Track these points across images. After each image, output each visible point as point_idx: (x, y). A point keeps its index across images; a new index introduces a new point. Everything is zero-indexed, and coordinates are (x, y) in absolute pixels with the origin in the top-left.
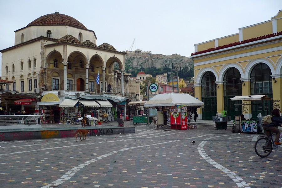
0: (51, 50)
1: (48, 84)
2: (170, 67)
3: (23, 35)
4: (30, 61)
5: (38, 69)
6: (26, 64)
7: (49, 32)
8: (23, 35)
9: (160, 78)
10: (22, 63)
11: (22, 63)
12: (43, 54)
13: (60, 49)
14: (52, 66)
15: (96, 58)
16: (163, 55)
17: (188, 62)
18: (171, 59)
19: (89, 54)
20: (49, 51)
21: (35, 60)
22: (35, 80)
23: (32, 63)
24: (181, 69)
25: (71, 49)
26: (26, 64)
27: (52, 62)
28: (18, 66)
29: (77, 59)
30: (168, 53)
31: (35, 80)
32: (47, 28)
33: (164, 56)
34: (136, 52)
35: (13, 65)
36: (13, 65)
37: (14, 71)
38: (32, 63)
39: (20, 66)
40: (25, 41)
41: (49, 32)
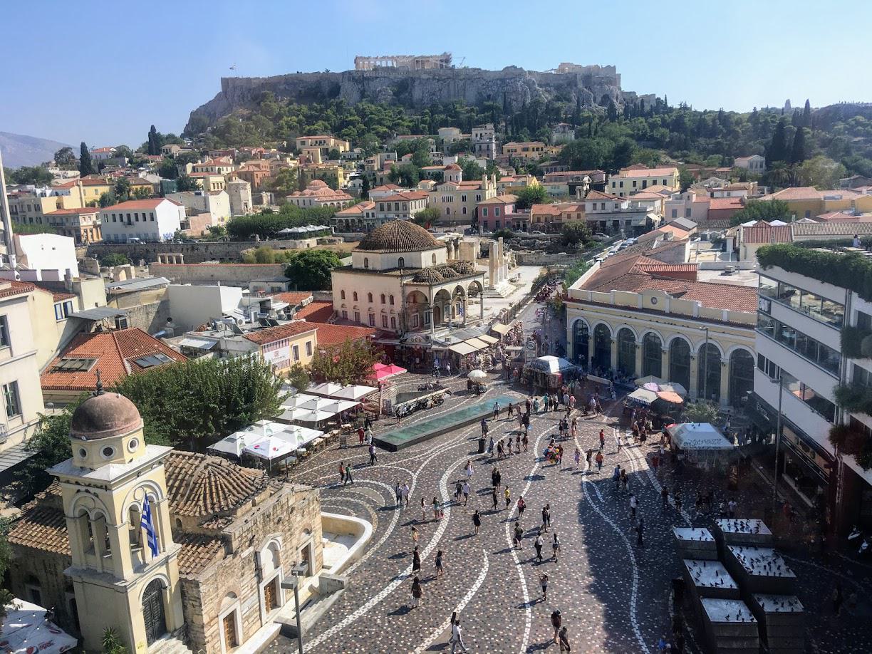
0: (414, 289)
1: (409, 324)
2: (500, 103)
3: (366, 260)
4: (383, 297)
5: (398, 307)
6: (377, 298)
7: (401, 260)
8: (366, 260)
9: (479, 136)
10: (370, 296)
11: (370, 296)
12: (403, 292)
13: (424, 290)
14: (411, 304)
15: (458, 289)
16: (483, 68)
17: (540, 86)
18: (503, 80)
19: (450, 288)
20: (409, 290)
21: (392, 298)
22: (393, 319)
23: (387, 299)
24: (524, 105)
25: (435, 290)
26: (377, 298)
27: (412, 300)
28: (363, 296)
29: (443, 295)
30: (492, 63)
31: (393, 319)
32: (398, 256)
33: (486, 72)
34: (417, 62)
35: (355, 294)
36: (355, 294)
37: (356, 299)
38: (387, 299)
39: (367, 297)
40: (370, 267)
41: (401, 260)
